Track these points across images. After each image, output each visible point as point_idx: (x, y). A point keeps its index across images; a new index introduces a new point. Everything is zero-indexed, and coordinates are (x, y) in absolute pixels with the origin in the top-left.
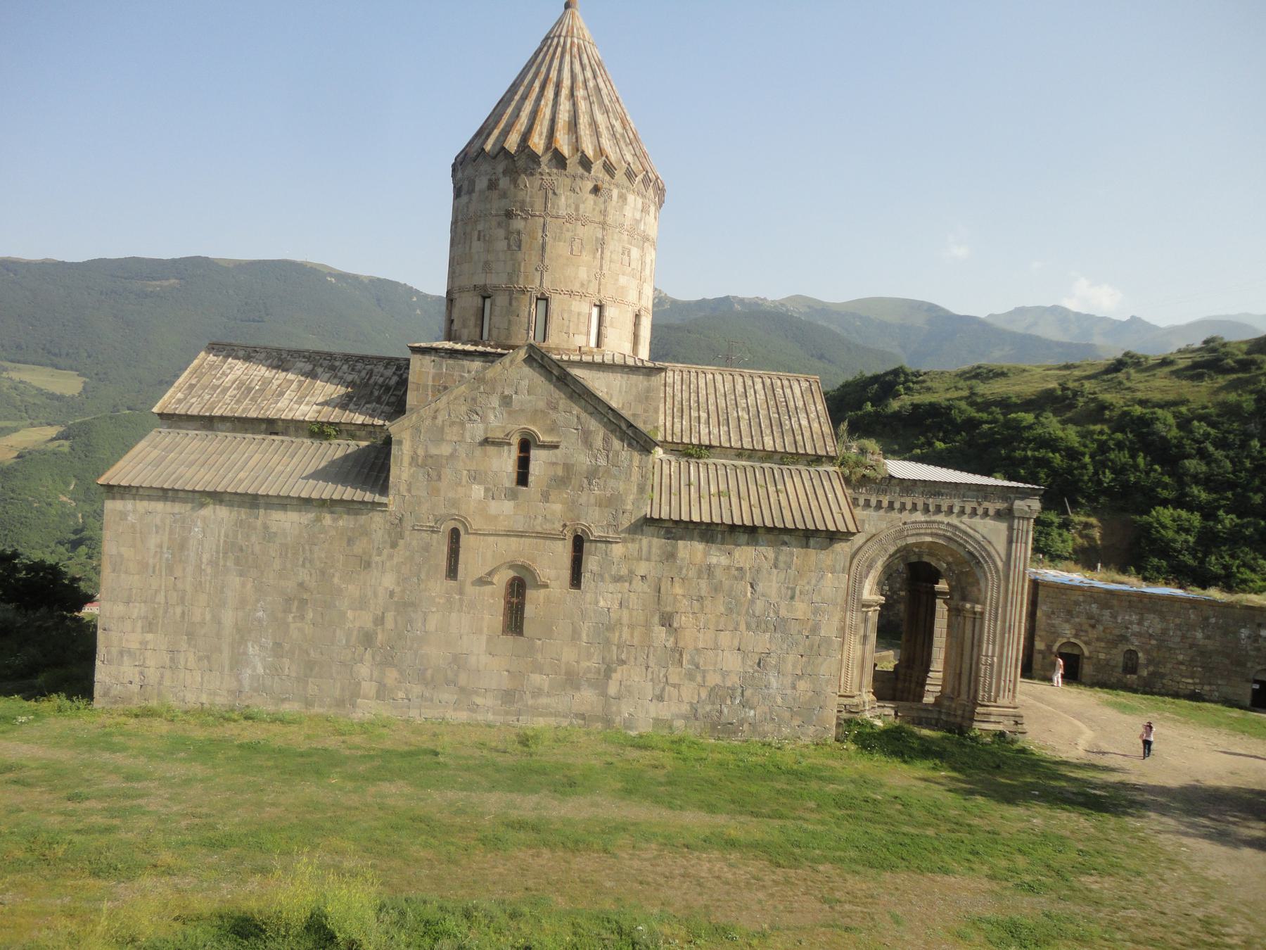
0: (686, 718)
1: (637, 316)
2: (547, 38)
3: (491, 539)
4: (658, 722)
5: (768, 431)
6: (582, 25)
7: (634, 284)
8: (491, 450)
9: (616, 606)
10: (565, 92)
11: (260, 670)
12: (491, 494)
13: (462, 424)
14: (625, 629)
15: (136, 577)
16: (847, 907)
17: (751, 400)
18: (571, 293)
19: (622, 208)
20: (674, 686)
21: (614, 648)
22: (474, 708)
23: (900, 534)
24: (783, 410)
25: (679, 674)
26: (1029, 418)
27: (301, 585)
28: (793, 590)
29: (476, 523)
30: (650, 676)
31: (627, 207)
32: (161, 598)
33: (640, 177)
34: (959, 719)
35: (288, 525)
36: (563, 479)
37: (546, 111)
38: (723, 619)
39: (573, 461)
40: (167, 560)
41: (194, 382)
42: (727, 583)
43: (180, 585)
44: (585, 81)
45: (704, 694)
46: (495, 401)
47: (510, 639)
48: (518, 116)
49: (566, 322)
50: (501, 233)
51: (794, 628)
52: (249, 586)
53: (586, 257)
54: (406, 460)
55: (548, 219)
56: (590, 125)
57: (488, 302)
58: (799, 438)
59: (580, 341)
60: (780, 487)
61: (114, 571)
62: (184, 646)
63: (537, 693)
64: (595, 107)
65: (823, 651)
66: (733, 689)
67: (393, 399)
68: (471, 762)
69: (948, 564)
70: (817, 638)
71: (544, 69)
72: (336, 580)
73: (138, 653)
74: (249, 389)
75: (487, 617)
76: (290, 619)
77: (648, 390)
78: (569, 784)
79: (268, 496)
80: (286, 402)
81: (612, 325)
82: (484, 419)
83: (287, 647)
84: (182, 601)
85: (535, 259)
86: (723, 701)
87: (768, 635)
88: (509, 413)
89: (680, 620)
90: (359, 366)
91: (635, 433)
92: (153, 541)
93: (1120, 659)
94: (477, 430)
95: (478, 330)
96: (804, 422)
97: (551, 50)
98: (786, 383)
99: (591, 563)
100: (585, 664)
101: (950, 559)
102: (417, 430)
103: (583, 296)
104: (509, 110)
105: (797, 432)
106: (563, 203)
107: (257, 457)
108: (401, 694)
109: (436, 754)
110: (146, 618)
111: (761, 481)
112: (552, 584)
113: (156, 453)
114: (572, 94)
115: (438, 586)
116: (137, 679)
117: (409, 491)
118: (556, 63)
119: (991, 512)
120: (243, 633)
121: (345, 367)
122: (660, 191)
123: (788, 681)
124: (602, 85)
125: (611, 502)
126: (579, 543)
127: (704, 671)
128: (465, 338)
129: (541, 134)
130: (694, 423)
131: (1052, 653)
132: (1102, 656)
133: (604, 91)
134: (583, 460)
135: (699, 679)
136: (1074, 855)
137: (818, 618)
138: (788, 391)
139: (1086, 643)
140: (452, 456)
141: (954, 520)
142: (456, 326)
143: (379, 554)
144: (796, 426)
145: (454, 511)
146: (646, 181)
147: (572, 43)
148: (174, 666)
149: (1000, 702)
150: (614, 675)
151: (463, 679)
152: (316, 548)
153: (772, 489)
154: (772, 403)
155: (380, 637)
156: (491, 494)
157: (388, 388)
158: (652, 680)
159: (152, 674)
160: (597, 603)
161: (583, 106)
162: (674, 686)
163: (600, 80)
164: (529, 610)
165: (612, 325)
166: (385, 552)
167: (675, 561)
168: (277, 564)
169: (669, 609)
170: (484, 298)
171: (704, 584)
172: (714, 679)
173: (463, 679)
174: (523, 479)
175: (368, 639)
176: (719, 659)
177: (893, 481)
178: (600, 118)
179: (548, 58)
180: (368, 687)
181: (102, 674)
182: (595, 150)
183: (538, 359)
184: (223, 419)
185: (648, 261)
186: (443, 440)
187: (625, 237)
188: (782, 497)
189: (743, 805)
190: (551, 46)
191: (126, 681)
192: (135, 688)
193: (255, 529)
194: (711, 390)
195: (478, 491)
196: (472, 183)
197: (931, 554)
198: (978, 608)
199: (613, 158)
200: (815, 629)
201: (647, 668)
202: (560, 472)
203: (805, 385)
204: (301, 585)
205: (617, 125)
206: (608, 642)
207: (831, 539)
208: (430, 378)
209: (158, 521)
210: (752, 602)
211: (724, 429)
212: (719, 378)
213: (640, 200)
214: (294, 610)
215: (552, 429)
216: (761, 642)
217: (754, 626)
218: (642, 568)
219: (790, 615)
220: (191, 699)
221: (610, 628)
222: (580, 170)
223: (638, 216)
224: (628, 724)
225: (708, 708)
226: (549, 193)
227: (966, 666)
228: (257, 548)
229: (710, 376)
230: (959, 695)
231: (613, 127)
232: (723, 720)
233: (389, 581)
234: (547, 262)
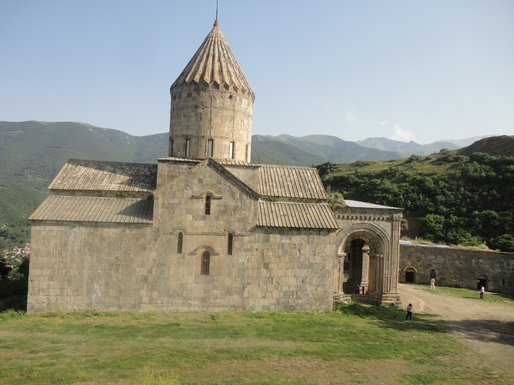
0: (275, 305)
1: (247, 146)
2: (207, 38)
3: (196, 236)
4: (264, 307)
5: (300, 190)
6: (221, 33)
7: (246, 133)
8: (195, 200)
9: (246, 261)
10: (216, 59)
11: (100, 294)
12: (195, 218)
13: (183, 190)
14: (250, 270)
15: (45, 258)
16: (356, 374)
17: (292, 178)
18: (222, 138)
19: (240, 104)
20: (270, 292)
21: (246, 278)
22: (190, 305)
23: (352, 229)
24: (304, 181)
25: (272, 287)
26: (378, 181)
27: (117, 258)
28: (315, 252)
29: (189, 230)
30: (260, 289)
31: (242, 104)
32: (56, 266)
33: (247, 92)
34: (376, 300)
35: (111, 234)
36: (224, 211)
37: (210, 66)
38: (288, 264)
39: (228, 204)
40: (59, 250)
41: (64, 175)
42: (289, 250)
43: (64, 260)
44: (224, 55)
45: (282, 295)
46: (196, 181)
47: (204, 277)
48: (198, 68)
49: (220, 149)
50: (193, 114)
51: (316, 267)
52: (94, 259)
53: (227, 123)
54: (160, 205)
55: (212, 108)
56: (227, 72)
57: (188, 141)
58: (312, 192)
59: (226, 156)
60: (307, 212)
61: (35, 256)
62: (66, 286)
63: (215, 298)
64: (229, 65)
65: (327, 275)
66: (293, 292)
67: (149, 181)
68: (194, 327)
69: (369, 239)
71: (207, 50)
72: (131, 256)
73: (46, 290)
74: (89, 178)
75: (194, 268)
76: (112, 273)
77: (254, 175)
78: (236, 334)
79: (102, 222)
80: (105, 183)
81: (238, 150)
82: (191, 188)
83: (111, 284)
84: (65, 267)
85: (207, 124)
86: (289, 297)
87: (306, 270)
88: (202, 186)
89: (272, 266)
90: (133, 167)
91: (252, 192)
92: (53, 243)
93: (429, 273)
94: (189, 193)
95: (185, 153)
96: (313, 186)
97: (210, 42)
98: (304, 171)
99: (236, 244)
100: (234, 285)
101: (370, 237)
102: (164, 193)
103: (227, 138)
104: (195, 66)
105: (311, 190)
106: (218, 102)
107: (95, 206)
108: (159, 301)
109: (179, 325)
110: (50, 275)
111: (299, 210)
112: (220, 253)
113: (51, 206)
114: (219, 60)
115: (174, 256)
116: (46, 301)
117: (161, 218)
118: (212, 47)
119: (385, 219)
120: (92, 279)
121: (127, 168)
122: (254, 97)
124: (230, 56)
125: (243, 220)
126: (231, 237)
127: (282, 286)
128: (179, 156)
129: (208, 75)
130: (271, 188)
131: (404, 272)
132: (422, 272)
133: (231, 59)
134: (232, 203)
135: (280, 289)
136: (432, 348)
137: (325, 262)
138: (305, 174)
139: (416, 268)
141: (371, 222)
142: (174, 151)
143: (149, 244)
144: (310, 188)
145: (180, 226)
146: (249, 93)
147: (218, 40)
148: (62, 294)
149: (391, 292)
150: (246, 289)
151: (185, 294)
152: (123, 243)
153: (304, 213)
154: (300, 179)
155: (150, 278)
156: (195, 218)
157: (147, 177)
158: (261, 290)
159: (53, 298)
160: (238, 260)
161: (224, 64)
162: (270, 292)
163: (229, 54)
164: (211, 265)
165: (238, 150)
166: (152, 243)
167: (269, 243)
168: (106, 250)
169: (267, 261)
170: (187, 140)
171: (280, 251)
172: (285, 289)
173: (185, 294)
174: (208, 212)
175: (145, 279)
176: (287, 280)
177: (349, 208)
178: (231, 69)
179: (209, 46)
180: (146, 299)
181: (30, 300)
182: (230, 82)
183: (213, 164)
184: (79, 191)
185: (250, 124)
186: (175, 197)
187: (242, 115)
188: (308, 215)
189: (304, 337)
190: (209, 41)
191: (41, 302)
192: (45, 305)
193: (97, 236)
194: (276, 175)
195: (190, 217)
196: (180, 94)
197: (363, 236)
198: (382, 256)
199: (237, 85)
200: (324, 267)
201: (259, 285)
202: (223, 209)
203: (311, 172)
204: (117, 258)
205: (237, 71)
206: (243, 276)
207: (329, 232)
208: (166, 172)
209: (55, 234)
210: (299, 257)
211: (283, 190)
212: (278, 169)
213: (247, 101)
214: (114, 268)
215: (219, 192)
216: (304, 273)
217: (300, 267)
218: (256, 246)
219: (314, 262)
220: (70, 308)
221: (244, 270)
222: (225, 90)
223: (246, 107)
224: (252, 309)
225: (283, 300)
226: (212, 98)
227: (378, 278)
228: (98, 244)
229: (275, 169)
230: (375, 290)
231: (236, 72)
232: (289, 305)
233: (154, 255)
234: (212, 125)
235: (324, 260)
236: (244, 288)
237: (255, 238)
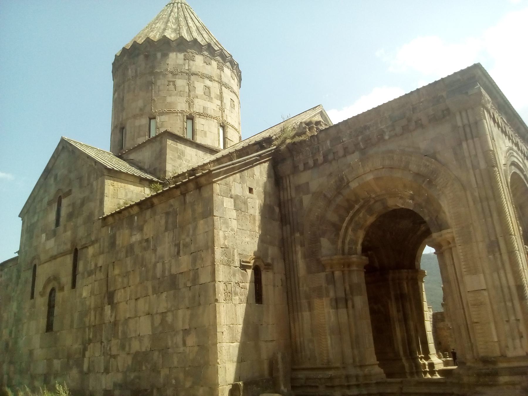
3: (46, 265)
21: (87, 330)
46: (52, 181)
51: (181, 281)
59: (141, 140)
66: (145, 354)
69: (412, 198)
70: (197, 287)
87: (164, 295)
89: (119, 296)
94: (46, 200)
123: (179, 339)
140: (38, 220)
160: (81, 295)
162: (115, 357)
169: (112, 289)
172: (136, 346)
200: (195, 279)
210: (155, 265)
216: (163, 303)
223: (181, 62)
235: (194, 261)
236: (85, 349)
237: (100, 247)
